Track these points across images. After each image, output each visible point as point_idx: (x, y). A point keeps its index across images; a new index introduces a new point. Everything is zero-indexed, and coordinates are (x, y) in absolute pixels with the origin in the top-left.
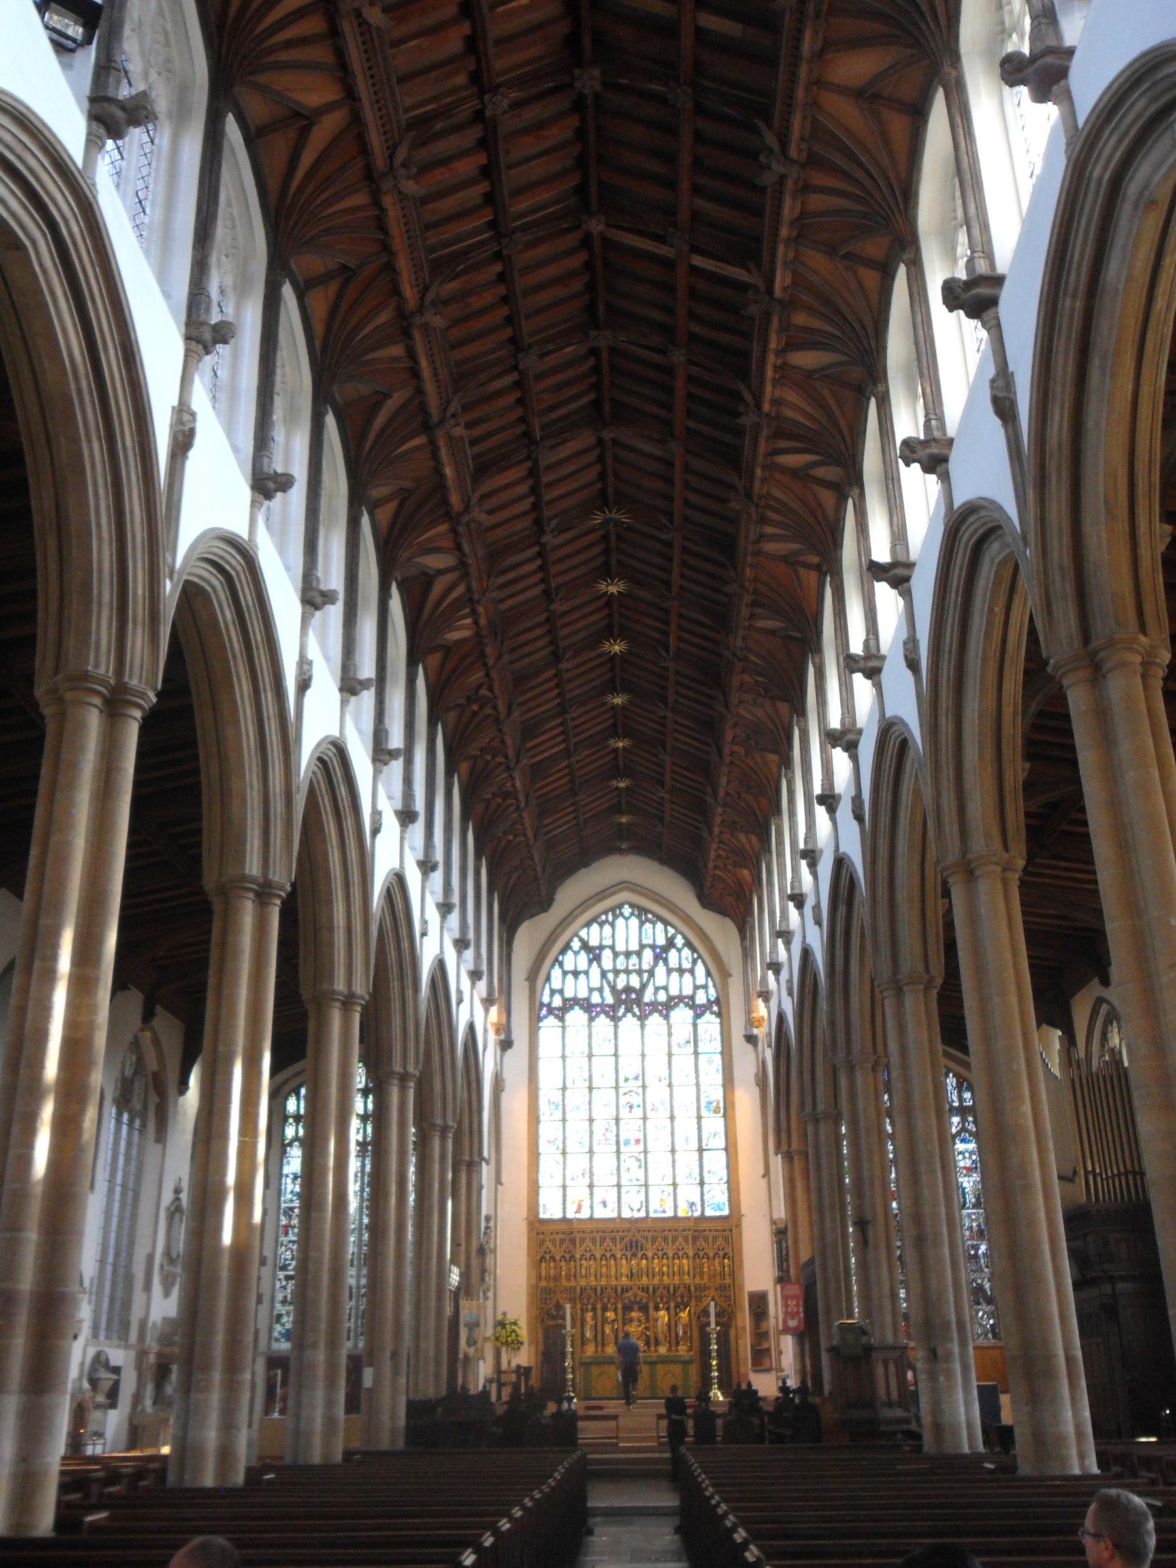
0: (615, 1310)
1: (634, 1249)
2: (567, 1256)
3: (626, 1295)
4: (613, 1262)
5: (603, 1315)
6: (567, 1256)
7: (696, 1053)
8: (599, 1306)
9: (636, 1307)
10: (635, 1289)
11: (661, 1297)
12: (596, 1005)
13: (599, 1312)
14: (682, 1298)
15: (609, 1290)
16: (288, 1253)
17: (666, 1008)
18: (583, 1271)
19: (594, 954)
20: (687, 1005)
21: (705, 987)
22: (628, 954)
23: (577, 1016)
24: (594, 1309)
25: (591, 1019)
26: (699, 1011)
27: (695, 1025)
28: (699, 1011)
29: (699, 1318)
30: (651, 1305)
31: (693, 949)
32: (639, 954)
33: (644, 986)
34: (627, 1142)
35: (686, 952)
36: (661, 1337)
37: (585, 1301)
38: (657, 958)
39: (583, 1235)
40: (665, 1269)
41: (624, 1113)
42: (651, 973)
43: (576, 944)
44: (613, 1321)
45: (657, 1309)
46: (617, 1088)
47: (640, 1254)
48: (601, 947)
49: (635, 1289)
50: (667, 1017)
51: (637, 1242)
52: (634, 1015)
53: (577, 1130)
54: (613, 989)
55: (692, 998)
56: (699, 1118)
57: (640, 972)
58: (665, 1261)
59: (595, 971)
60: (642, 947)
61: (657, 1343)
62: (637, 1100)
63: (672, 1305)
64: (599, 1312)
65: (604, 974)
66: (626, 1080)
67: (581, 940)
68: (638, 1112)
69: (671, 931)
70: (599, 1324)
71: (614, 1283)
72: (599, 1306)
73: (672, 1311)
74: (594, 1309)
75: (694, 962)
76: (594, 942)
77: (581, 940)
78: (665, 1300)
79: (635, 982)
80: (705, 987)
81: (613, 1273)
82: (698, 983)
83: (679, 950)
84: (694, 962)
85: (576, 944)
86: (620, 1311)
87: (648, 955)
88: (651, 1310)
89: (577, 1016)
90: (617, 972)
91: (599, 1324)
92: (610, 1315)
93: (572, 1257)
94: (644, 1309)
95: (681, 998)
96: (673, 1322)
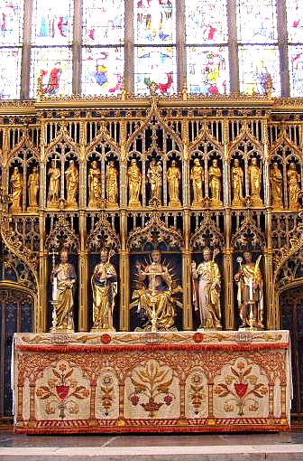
0: (115, 261)
1: (154, 146)
2: (25, 163)
3: (137, 230)
4: (112, 171)
5: (90, 273)
6: (25, 163)
8: (83, 253)
9: (156, 254)
10: (155, 219)
11: (208, 237)
13: (83, 263)
14: (249, 236)
15: (103, 221)
18: (53, 188)
24: (74, 259)
29: (280, 276)
30: (187, 251)
36: (205, 310)
37: (55, 242)
39: (53, 121)
40: (215, 184)
44: (110, 280)
45: (198, 258)
47: (165, 158)
49: (155, 219)
51: (159, 133)
58: (214, 170)
61: (197, 322)
63: (228, 250)
64: (83, 263)
70: (83, 286)
71: (113, 207)
72: (83, 253)
73: (227, 262)
74: (74, 259)
78: (214, 240)
81: (112, 191)
86: (124, 263)
88: (186, 261)
91: (83, 286)
92: (105, 270)
93: (34, 164)
94: (173, 260)
96: (229, 285)
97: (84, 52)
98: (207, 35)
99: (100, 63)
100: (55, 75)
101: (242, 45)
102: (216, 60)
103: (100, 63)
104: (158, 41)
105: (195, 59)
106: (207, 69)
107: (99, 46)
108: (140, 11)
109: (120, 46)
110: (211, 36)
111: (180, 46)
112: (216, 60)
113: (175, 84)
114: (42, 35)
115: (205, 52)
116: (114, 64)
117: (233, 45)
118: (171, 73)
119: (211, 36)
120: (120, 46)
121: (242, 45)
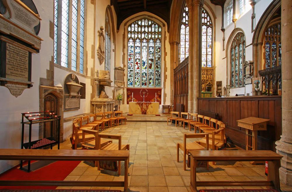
7: (207, 35)
16: (131, 65)
27: (207, 29)
35: (206, 14)
56: (207, 48)
75: (207, 17)
80: (209, 22)
82: (208, 20)
84: (207, 17)
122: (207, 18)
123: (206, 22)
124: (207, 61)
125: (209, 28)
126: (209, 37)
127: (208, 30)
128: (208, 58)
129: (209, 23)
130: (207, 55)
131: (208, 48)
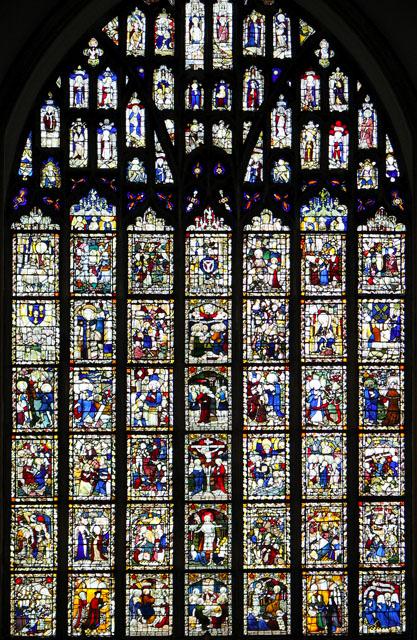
12: (138, 187)
17: (289, 201)
19: (135, 77)
20: (335, 194)
21: (377, 155)
22: (209, 77)
23: (94, 214)
25: (125, 218)
26: (361, 207)
28: (361, 207)
31: (354, 75)
32: (234, 78)
33: (243, 149)
34: (198, 482)
35: (336, 79)
38: (272, 91)
41: (193, 417)
42: (262, 123)
43: (94, 53)
46: (178, 367)
48: (151, 61)
50: (291, 219)
52: (219, 212)
53: (92, 450)
54: (175, 154)
55: (350, 174)
57: (234, 120)
59: (135, 113)
60: (242, 62)
62: (223, 391)
65: (154, 119)
66: (199, 350)
67: (105, 42)
68: (223, 420)
69: (308, 30)
75: (356, 103)
76: (135, 46)
77: (105, 42)
79: (222, 135)
80: (377, 155)
82: (363, 144)
83: (323, 75)
84: (356, 103)
85: (94, 53)
87: (254, 79)
89: (94, 214)
90: (182, 116)
95: (323, 175)
97: (129, 581)
98: (266, 558)
99: (147, 591)
100: (98, 603)
101: (308, 570)
102: (277, 589)
103: (147, 591)
104: (212, 565)
105: (254, 588)
106: (267, 599)
107: (144, 572)
108: (192, 527)
109: (169, 571)
110: (271, 561)
111: (237, 571)
112: (277, 589)
113: (229, 619)
114: (80, 556)
115: (264, 580)
116: (162, 595)
117: (297, 571)
118: (226, 604)
119: (271, 561)
120: (169, 571)
121: (308, 570)
122: (118, 117)
123: (108, 159)
124: (353, 568)
125: (380, 220)
126: (380, 316)
127: (367, 243)
128: (365, 534)
129: (381, 166)
130: (354, 500)
131: (369, 424)
